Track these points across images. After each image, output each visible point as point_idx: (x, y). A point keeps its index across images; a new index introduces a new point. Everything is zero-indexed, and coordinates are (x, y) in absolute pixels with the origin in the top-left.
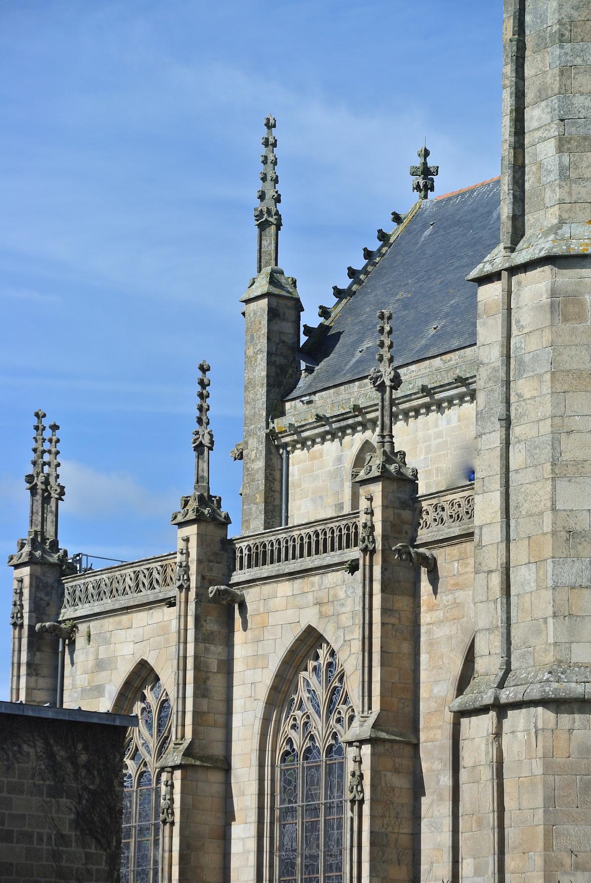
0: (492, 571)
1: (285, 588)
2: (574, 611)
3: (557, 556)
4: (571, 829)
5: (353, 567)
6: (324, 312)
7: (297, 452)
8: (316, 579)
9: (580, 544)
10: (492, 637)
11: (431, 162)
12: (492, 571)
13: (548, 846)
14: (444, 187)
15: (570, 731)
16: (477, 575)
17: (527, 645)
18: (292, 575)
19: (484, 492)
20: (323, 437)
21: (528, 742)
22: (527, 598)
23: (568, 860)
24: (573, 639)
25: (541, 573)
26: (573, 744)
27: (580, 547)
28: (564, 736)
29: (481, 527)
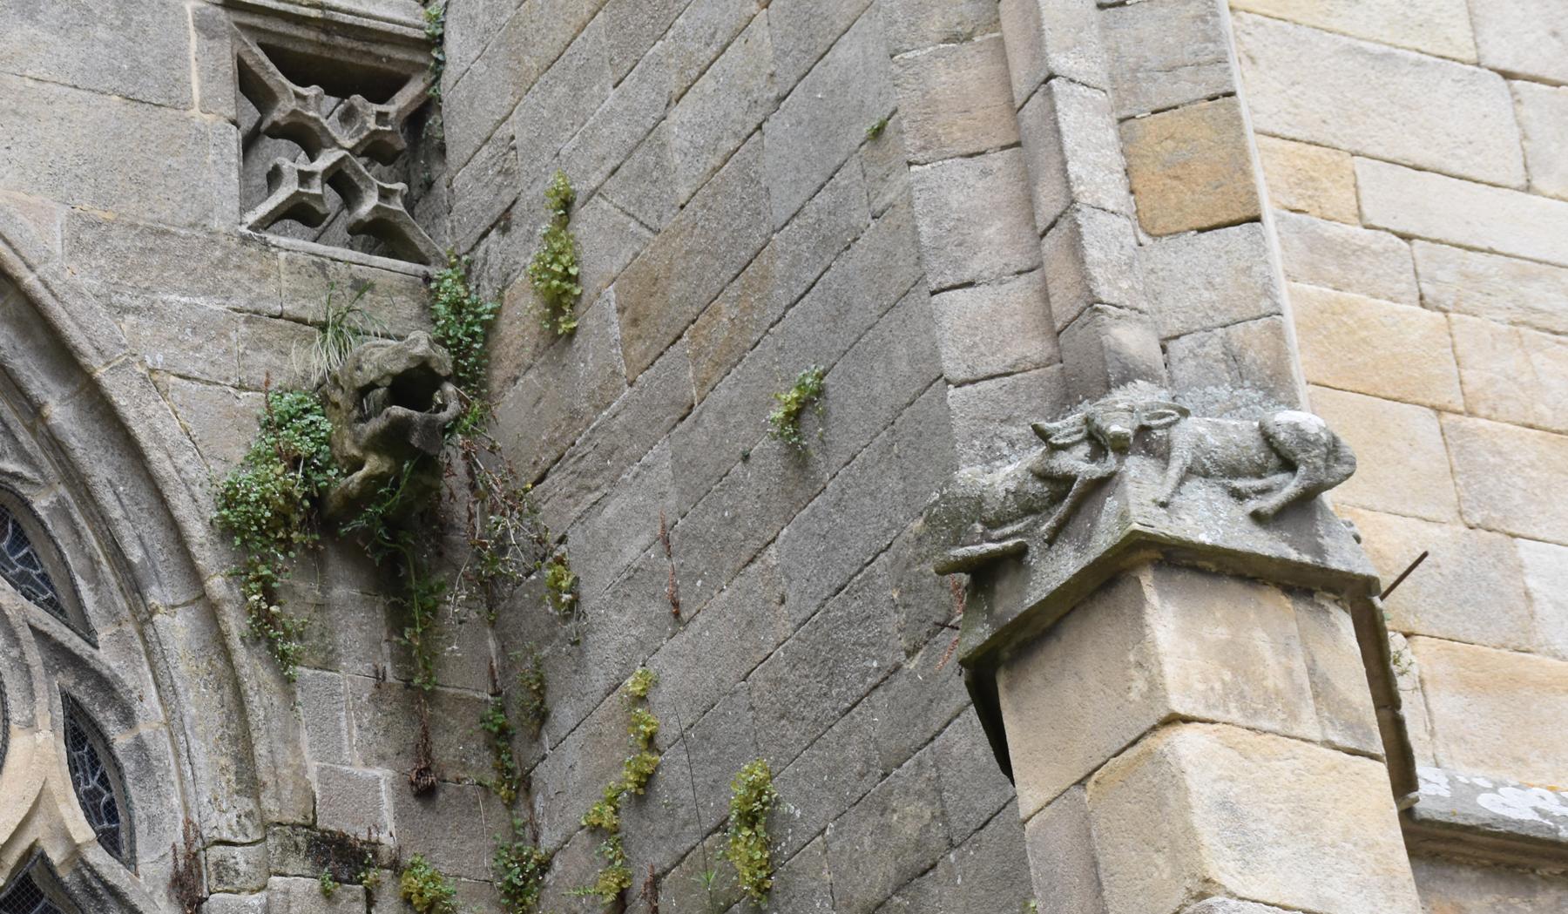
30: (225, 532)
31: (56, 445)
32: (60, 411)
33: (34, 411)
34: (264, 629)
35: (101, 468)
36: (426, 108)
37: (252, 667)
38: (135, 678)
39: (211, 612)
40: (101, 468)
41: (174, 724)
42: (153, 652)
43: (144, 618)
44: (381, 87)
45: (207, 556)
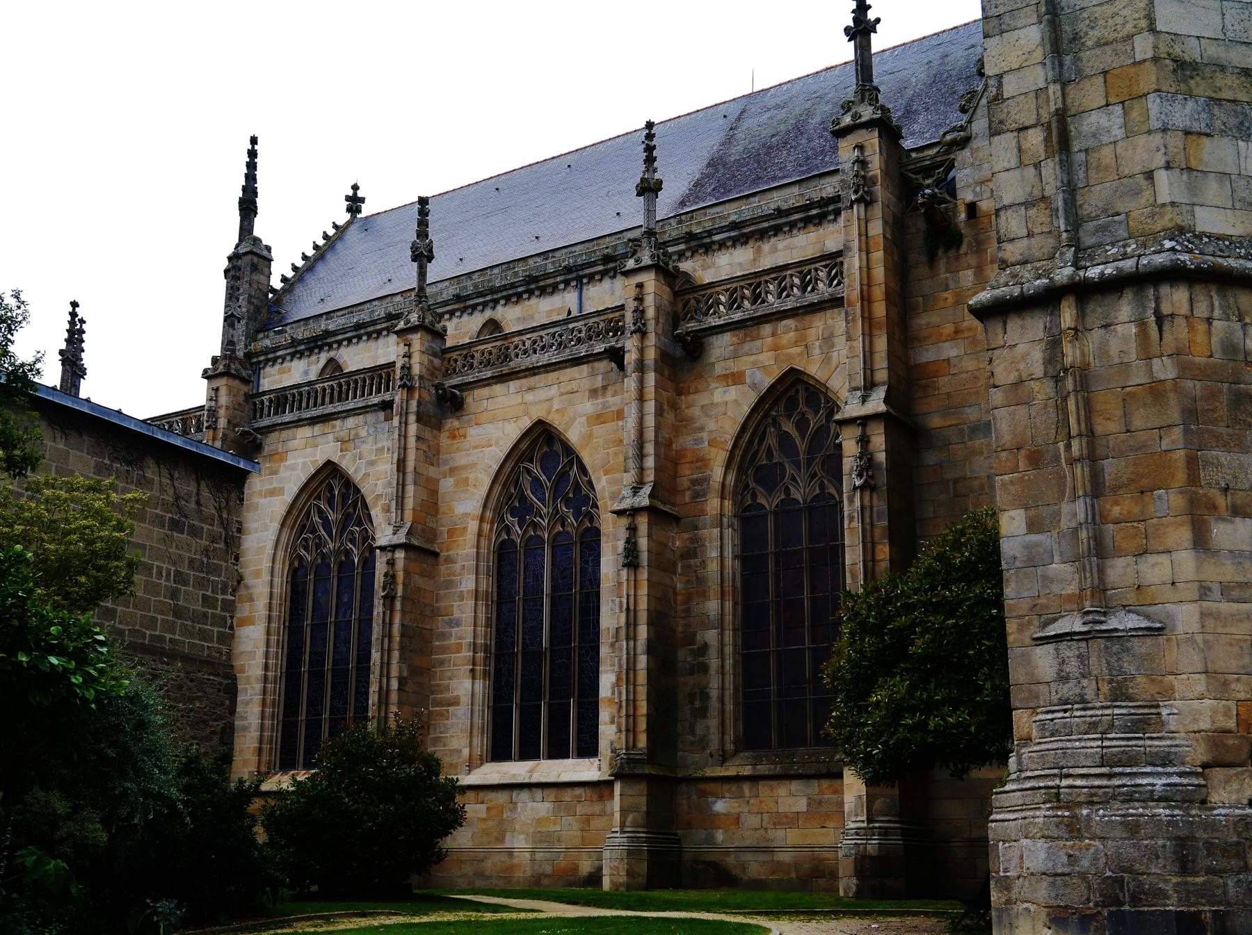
0: (1026, 128)
1: (304, 432)
2: (1193, 164)
3: (1164, 89)
4: (1223, 456)
5: (387, 406)
6: (284, 279)
7: (268, 369)
8: (338, 423)
9: (1192, 78)
11: (360, 194)
12: (1026, 128)
13: (1193, 479)
14: (367, 210)
15: (1209, 321)
16: (996, 139)
17: (1110, 212)
18: (313, 421)
19: (1002, 32)
20: (293, 356)
22: (1107, 152)
23: (1222, 502)
24: (1195, 200)
25: (1135, 114)
26: (1215, 340)
28: (1202, 327)
29: (1000, 77)
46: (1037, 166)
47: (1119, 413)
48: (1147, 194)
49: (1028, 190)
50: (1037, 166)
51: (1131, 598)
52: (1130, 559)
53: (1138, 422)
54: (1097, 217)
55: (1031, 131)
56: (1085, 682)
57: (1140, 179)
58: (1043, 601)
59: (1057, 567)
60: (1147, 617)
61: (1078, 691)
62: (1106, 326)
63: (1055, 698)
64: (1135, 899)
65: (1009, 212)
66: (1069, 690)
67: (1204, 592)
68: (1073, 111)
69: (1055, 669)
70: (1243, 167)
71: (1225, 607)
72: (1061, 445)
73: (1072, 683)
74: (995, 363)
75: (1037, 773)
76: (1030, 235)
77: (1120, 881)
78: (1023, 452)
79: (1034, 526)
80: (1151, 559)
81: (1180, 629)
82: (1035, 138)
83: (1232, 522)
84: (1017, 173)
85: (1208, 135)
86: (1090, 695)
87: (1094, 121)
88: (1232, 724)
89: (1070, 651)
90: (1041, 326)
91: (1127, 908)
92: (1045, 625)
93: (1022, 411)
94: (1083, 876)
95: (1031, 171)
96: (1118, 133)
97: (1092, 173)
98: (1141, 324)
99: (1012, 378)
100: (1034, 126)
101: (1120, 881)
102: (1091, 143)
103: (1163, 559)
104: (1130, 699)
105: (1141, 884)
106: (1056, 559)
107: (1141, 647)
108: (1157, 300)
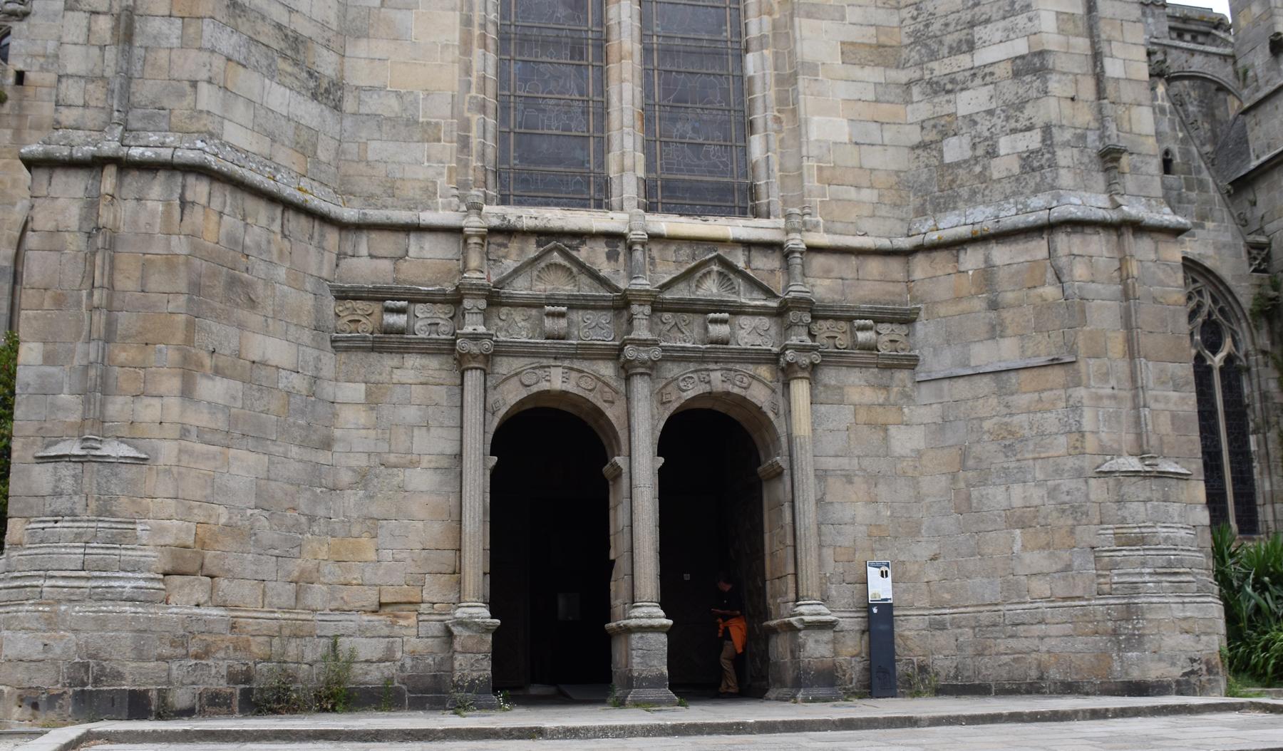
0: (98, 13)
2: (229, 86)
3: (218, 18)
4: (215, 327)
9: (240, 17)
10: (91, 87)
12: (98, 13)
13: (189, 340)
15: (221, 214)
16: (70, 14)
17: (157, 105)
21: (167, 214)
22: (163, 56)
23: (208, 362)
24: (226, 115)
25: (191, 30)
26: (223, 230)
27: (239, 21)
28: (214, 218)
30: (1251, 314)
31: (1229, 303)
32: (1230, 299)
33: (1227, 299)
34: (1256, 327)
35: (1235, 306)
36: (1269, 252)
37: (1254, 331)
38: (1239, 331)
39: (1249, 324)
40: (1235, 306)
41: (1244, 336)
42: (1241, 328)
43: (1240, 324)
44: (1263, 249)
45: (1249, 317)
46: (102, 48)
47: (138, 274)
48: (189, 100)
49: (90, 66)
50: (102, 48)
51: (124, 432)
52: (129, 399)
53: (152, 285)
54: (145, 107)
55: (101, 18)
56: (76, 498)
57: (186, 85)
58: (48, 425)
59: (65, 397)
60: (136, 448)
61: (69, 505)
62: (139, 200)
63: (48, 510)
64: (97, 681)
65: (70, 81)
66: (61, 504)
67: (184, 433)
68: (141, 12)
69: (51, 485)
70: (265, 99)
71: (199, 447)
72: (84, 293)
73: (65, 498)
74: (37, 209)
75: (24, 574)
76: (85, 106)
77: (86, 666)
78: (50, 293)
79: (49, 359)
80: (147, 401)
81: (161, 461)
82: (104, 25)
83: (213, 379)
84: (83, 49)
85: (244, 66)
86: (79, 508)
87: (156, 25)
88: (190, 541)
89: (66, 470)
90: (83, 187)
91: (89, 688)
92: (47, 446)
93: (53, 256)
94: (54, 661)
95: (95, 52)
96: (175, 42)
97: (148, 69)
98: (168, 203)
99: (50, 226)
100: (105, 13)
101: (86, 666)
102: (150, 43)
103: (156, 402)
104: (113, 515)
105: (103, 668)
106: (65, 390)
107: (128, 472)
108: (184, 187)
